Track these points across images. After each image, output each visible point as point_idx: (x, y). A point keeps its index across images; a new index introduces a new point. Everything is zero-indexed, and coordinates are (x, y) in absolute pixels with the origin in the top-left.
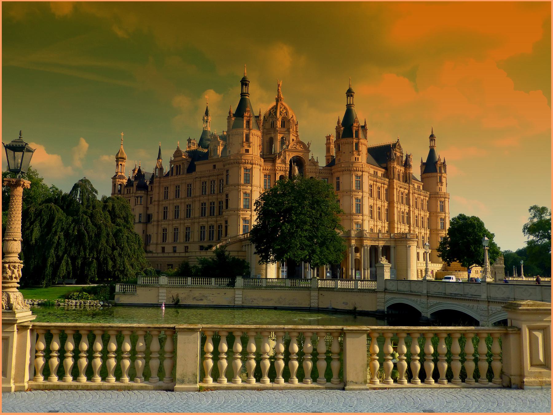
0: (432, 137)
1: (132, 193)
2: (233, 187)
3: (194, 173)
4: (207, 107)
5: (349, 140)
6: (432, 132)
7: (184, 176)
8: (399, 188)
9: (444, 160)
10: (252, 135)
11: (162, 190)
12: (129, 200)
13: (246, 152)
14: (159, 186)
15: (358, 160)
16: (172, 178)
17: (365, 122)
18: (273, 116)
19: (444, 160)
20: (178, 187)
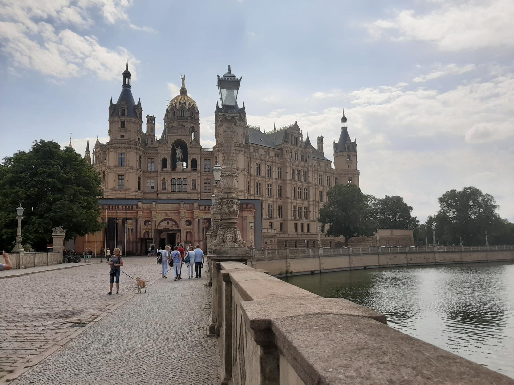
0: (344, 119)
8: (294, 167)
9: (355, 139)
10: (127, 122)
13: (121, 138)
17: (244, 105)
18: (174, 106)
19: (355, 139)
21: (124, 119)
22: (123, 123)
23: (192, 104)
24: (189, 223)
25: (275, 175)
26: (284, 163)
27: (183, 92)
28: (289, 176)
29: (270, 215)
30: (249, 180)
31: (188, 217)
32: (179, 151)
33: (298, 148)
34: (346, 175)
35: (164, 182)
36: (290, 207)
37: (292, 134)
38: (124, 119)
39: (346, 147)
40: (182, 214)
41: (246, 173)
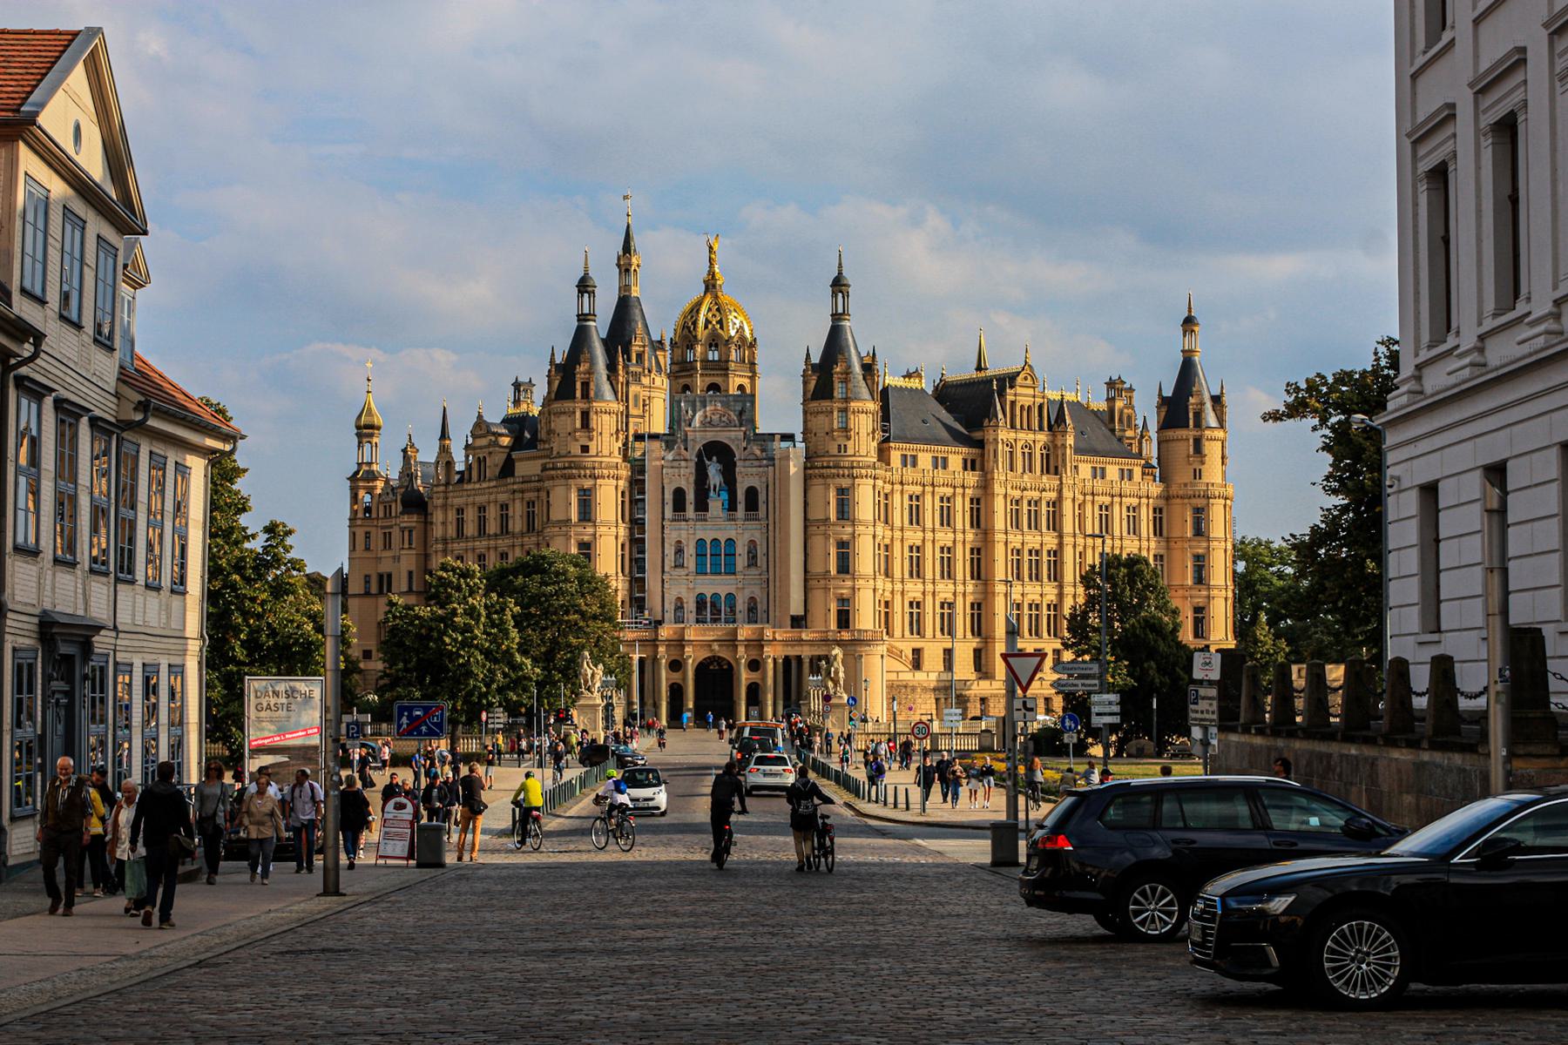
0: (1189, 323)
1: (396, 517)
2: (557, 529)
3: (510, 480)
4: (628, 227)
5: (825, 404)
6: (1190, 308)
7: (493, 484)
9: (1222, 387)
10: (596, 413)
11: (452, 516)
12: (390, 533)
14: (445, 507)
15: (845, 452)
16: (470, 486)
18: (690, 332)
19: (1222, 387)
20: (482, 509)
21: (587, 406)
22: (586, 416)
23: (737, 322)
24: (754, 665)
25: (961, 517)
26: (986, 485)
27: (710, 285)
28: (999, 523)
29: (948, 627)
30: (887, 541)
31: (754, 654)
32: (714, 476)
33: (1031, 436)
34: (1186, 501)
35: (679, 551)
36: (999, 606)
37: (1013, 398)
38: (587, 406)
39: (1191, 415)
40: (741, 650)
41: (880, 530)
